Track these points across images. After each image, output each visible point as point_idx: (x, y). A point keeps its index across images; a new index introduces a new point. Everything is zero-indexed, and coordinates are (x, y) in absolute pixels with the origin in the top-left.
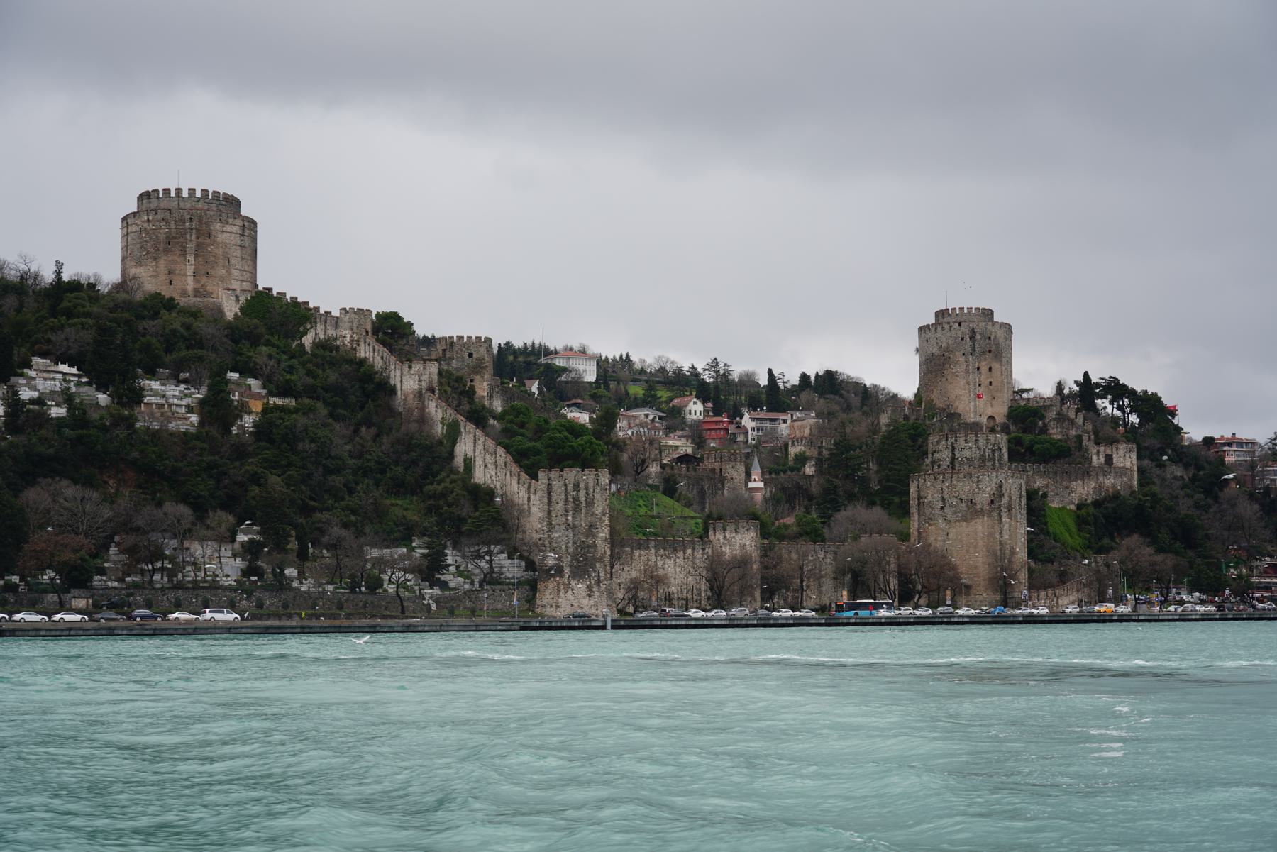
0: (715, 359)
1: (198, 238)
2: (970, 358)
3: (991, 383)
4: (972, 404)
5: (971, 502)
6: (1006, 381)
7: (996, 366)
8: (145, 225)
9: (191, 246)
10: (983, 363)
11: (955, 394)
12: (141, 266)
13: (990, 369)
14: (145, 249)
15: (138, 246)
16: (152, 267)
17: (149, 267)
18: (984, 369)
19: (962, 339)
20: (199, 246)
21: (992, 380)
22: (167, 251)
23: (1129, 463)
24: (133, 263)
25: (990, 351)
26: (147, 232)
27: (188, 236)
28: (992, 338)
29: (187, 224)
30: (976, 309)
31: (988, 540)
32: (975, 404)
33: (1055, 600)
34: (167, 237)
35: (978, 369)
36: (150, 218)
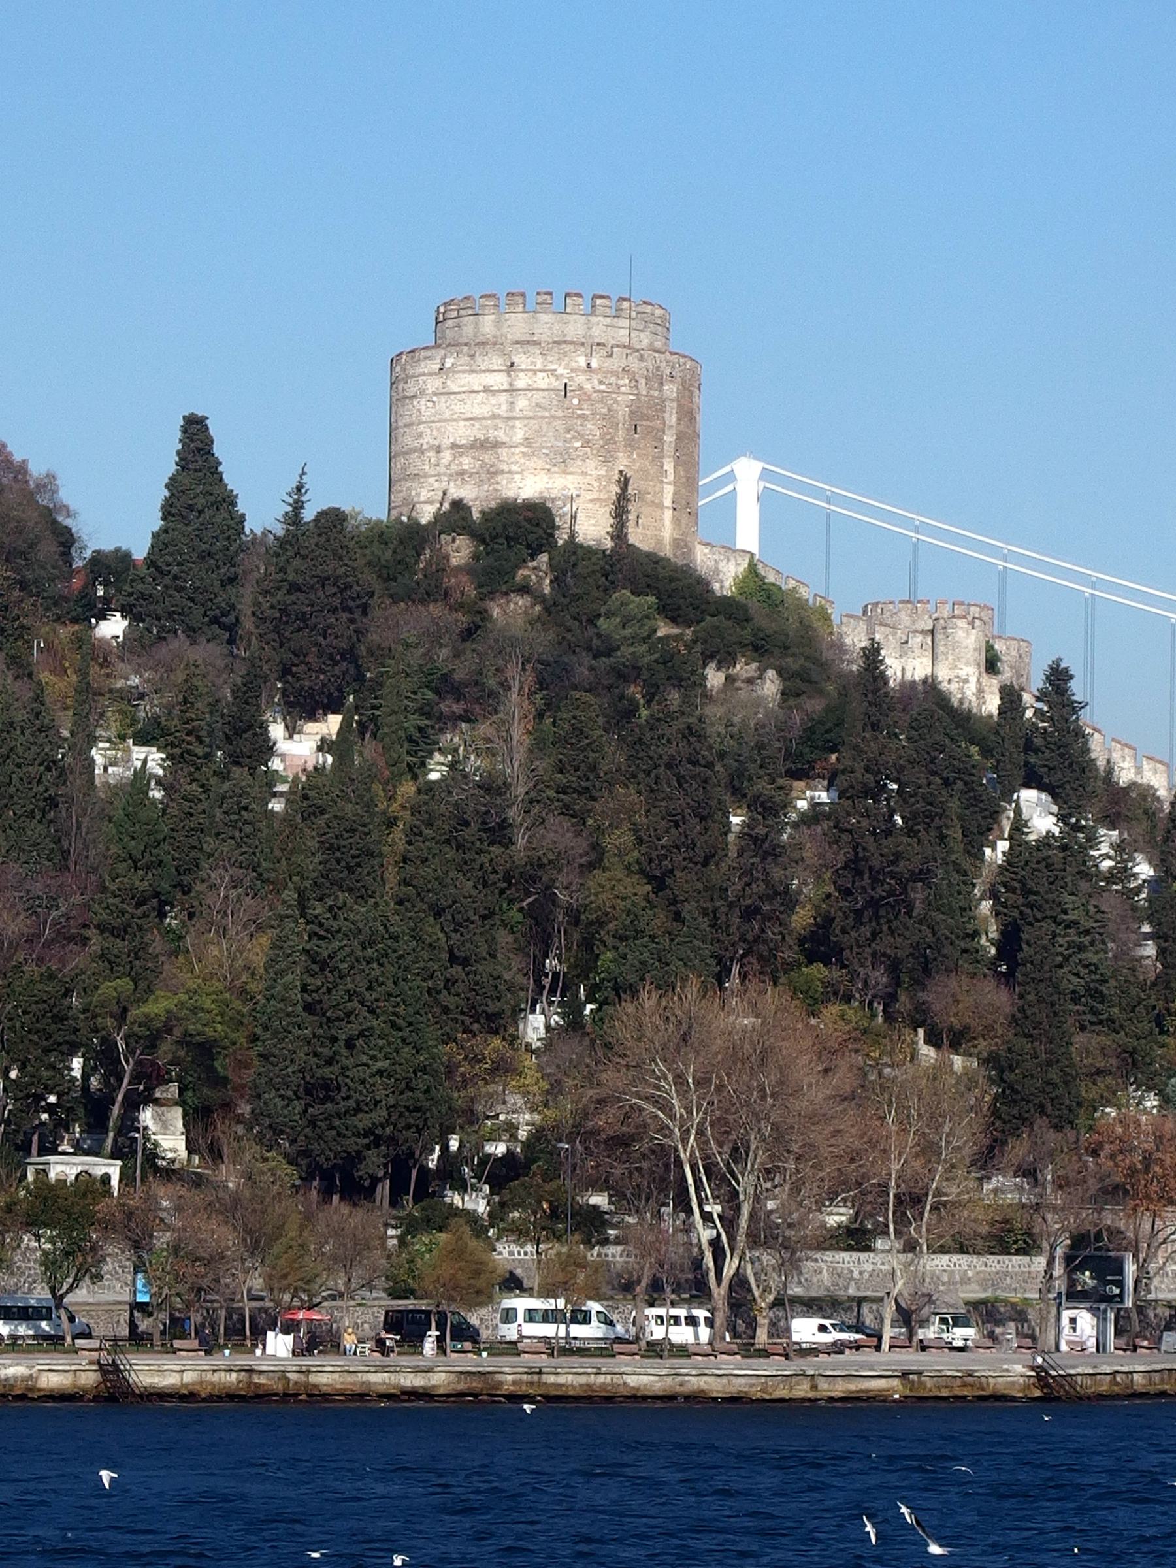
1: (679, 419)
8: (581, 379)
9: (669, 438)
12: (565, 472)
14: (580, 436)
15: (558, 424)
16: (598, 479)
17: (588, 479)
20: (680, 437)
22: (630, 445)
24: (539, 463)
26: (585, 397)
27: (666, 415)
29: (666, 388)
34: (632, 412)
36: (594, 364)
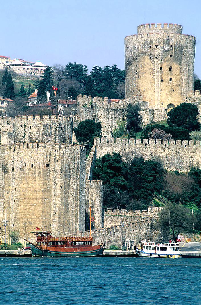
0: (75, 62)
3: (171, 79)
4: (156, 94)
7: (175, 66)
10: (165, 64)
11: (144, 87)
13: (170, 69)
18: (166, 69)
21: (172, 77)
28: (173, 46)
32: (158, 95)
35: (161, 68)
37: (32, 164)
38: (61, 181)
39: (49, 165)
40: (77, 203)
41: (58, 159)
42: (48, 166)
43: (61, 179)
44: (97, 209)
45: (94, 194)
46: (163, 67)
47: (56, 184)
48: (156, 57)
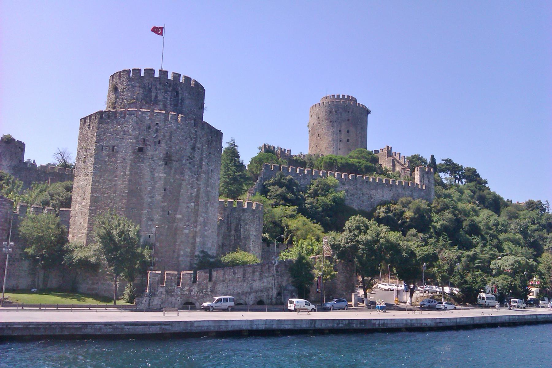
2: (335, 124)
3: (348, 140)
5: (113, 151)
6: (360, 140)
7: (352, 129)
13: (348, 132)
18: (344, 132)
19: (330, 112)
21: (349, 138)
23: (427, 182)
25: (348, 120)
28: (350, 112)
30: (343, 95)
31: (128, 201)
33: (209, 286)
35: (340, 131)
37: (114, 147)
38: (165, 178)
39: (142, 148)
40: (196, 222)
41: (160, 138)
42: (141, 150)
43: (165, 175)
44: (253, 242)
45: (248, 220)
46: (341, 129)
47: (155, 183)
48: (336, 122)
